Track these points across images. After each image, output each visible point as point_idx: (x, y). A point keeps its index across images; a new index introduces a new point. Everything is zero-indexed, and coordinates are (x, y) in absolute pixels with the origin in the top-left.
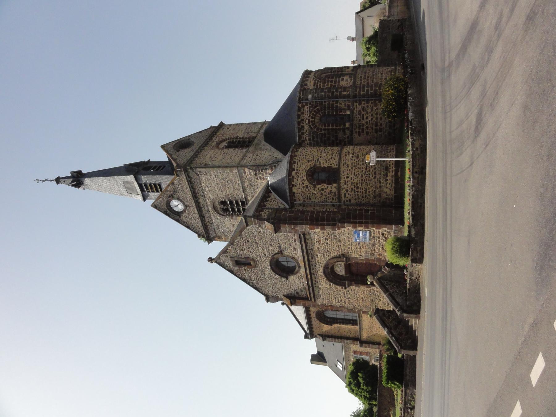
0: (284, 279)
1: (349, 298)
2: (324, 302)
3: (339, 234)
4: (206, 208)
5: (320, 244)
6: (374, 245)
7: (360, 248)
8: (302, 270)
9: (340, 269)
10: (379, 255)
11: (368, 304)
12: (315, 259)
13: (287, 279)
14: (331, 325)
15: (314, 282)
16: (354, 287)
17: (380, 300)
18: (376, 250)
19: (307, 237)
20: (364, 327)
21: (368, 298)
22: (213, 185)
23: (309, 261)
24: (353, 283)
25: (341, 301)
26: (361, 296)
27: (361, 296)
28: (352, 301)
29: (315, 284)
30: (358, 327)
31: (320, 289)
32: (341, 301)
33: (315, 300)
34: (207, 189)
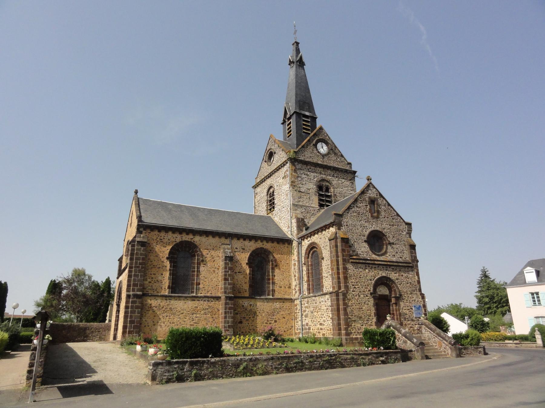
0: (365, 238)
1: (359, 296)
2: (349, 271)
3: (416, 294)
4: (323, 172)
5: (406, 277)
6: (413, 320)
7: (408, 309)
8: (374, 257)
9: (383, 291)
10: (406, 325)
11: (356, 314)
12: (393, 271)
13: (365, 241)
14: (167, 258)
15: (371, 266)
16: (373, 302)
17: (362, 325)
18: (409, 322)
19: (410, 269)
20: (173, 302)
21: (363, 313)
22: (344, 189)
23: (390, 266)
24: (377, 301)
25: (355, 288)
26: (364, 308)
27: (364, 308)
28: (356, 298)
29: (369, 266)
30: (167, 294)
31: (365, 270)
32: (355, 288)
33: (352, 262)
34: (340, 182)
